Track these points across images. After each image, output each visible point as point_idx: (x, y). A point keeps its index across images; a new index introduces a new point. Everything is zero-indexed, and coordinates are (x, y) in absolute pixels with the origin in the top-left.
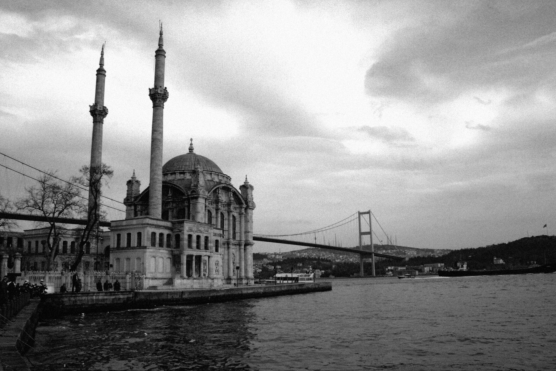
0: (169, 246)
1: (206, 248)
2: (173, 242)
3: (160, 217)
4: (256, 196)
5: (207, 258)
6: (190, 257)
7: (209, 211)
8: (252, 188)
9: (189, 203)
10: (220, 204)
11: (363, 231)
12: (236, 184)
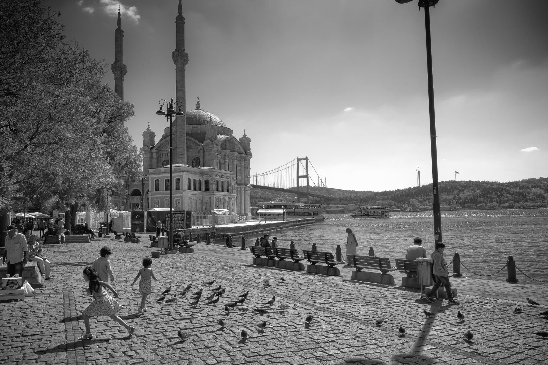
2: (203, 187)
4: (253, 148)
6: (217, 199)
11: (300, 175)
12: (238, 135)
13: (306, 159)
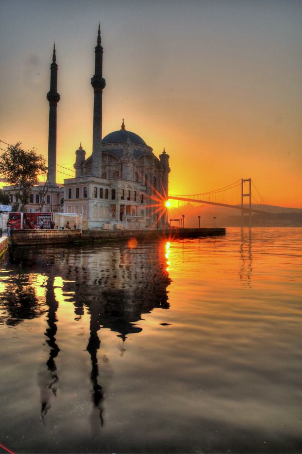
0: (107, 197)
1: (135, 200)
2: (110, 196)
3: (101, 176)
5: (135, 208)
6: (122, 206)
7: (136, 173)
8: (168, 157)
9: (122, 167)
10: (144, 168)
12: (157, 153)
13: (250, 180)
